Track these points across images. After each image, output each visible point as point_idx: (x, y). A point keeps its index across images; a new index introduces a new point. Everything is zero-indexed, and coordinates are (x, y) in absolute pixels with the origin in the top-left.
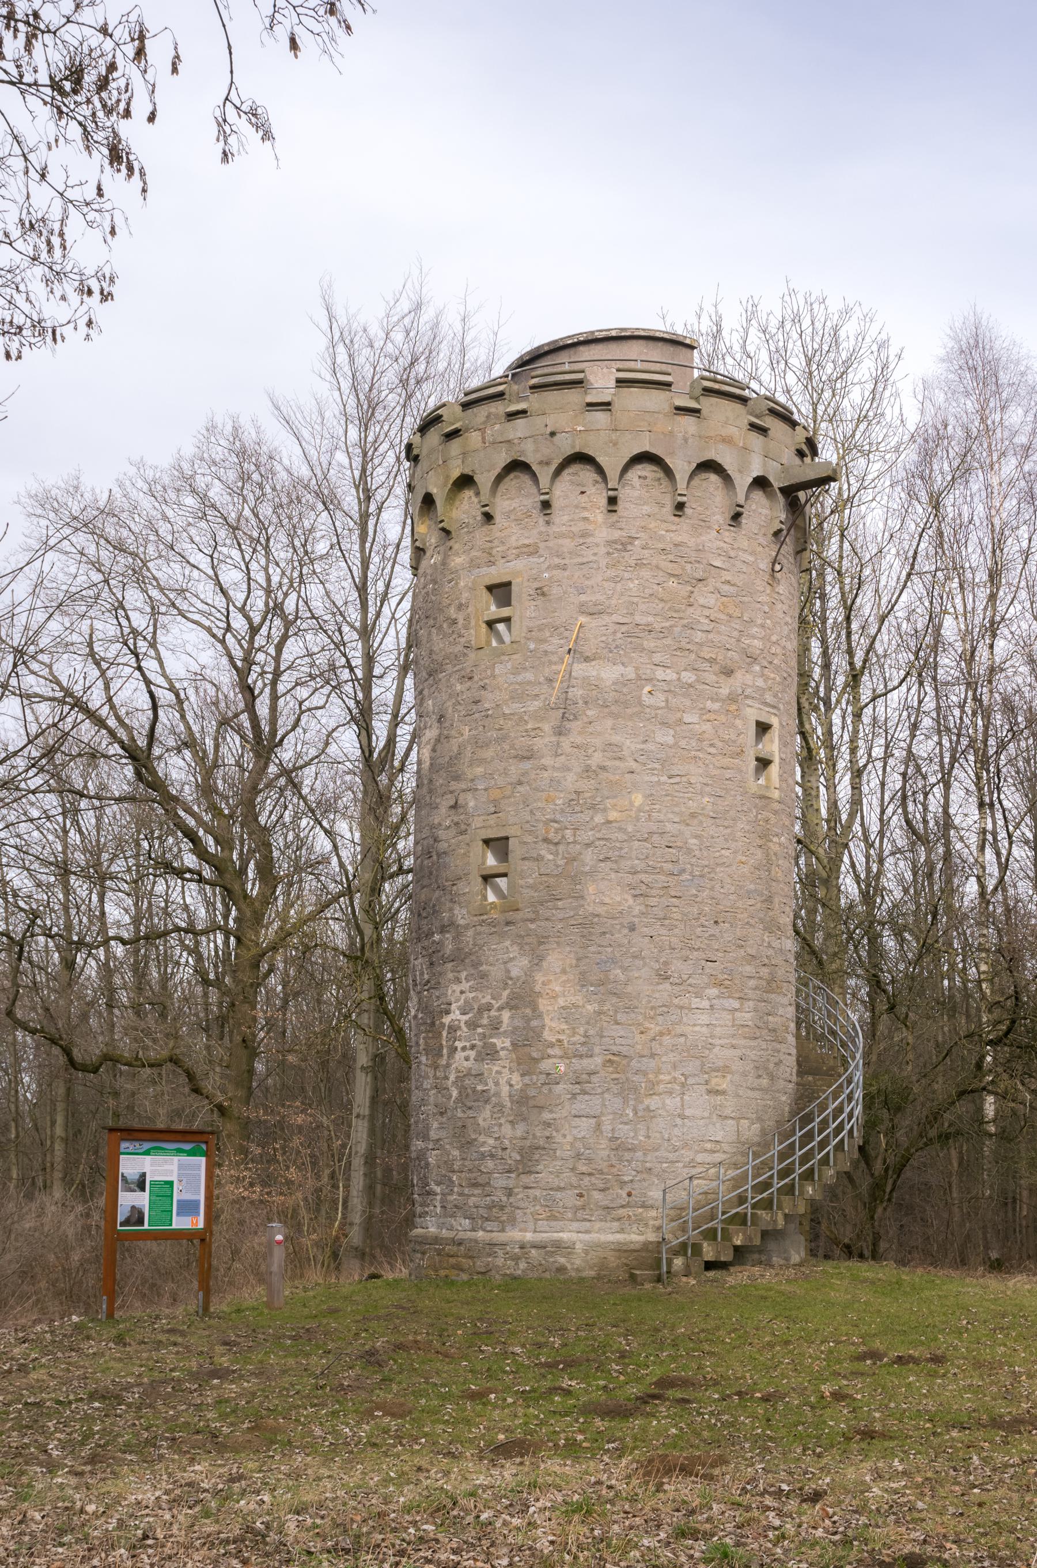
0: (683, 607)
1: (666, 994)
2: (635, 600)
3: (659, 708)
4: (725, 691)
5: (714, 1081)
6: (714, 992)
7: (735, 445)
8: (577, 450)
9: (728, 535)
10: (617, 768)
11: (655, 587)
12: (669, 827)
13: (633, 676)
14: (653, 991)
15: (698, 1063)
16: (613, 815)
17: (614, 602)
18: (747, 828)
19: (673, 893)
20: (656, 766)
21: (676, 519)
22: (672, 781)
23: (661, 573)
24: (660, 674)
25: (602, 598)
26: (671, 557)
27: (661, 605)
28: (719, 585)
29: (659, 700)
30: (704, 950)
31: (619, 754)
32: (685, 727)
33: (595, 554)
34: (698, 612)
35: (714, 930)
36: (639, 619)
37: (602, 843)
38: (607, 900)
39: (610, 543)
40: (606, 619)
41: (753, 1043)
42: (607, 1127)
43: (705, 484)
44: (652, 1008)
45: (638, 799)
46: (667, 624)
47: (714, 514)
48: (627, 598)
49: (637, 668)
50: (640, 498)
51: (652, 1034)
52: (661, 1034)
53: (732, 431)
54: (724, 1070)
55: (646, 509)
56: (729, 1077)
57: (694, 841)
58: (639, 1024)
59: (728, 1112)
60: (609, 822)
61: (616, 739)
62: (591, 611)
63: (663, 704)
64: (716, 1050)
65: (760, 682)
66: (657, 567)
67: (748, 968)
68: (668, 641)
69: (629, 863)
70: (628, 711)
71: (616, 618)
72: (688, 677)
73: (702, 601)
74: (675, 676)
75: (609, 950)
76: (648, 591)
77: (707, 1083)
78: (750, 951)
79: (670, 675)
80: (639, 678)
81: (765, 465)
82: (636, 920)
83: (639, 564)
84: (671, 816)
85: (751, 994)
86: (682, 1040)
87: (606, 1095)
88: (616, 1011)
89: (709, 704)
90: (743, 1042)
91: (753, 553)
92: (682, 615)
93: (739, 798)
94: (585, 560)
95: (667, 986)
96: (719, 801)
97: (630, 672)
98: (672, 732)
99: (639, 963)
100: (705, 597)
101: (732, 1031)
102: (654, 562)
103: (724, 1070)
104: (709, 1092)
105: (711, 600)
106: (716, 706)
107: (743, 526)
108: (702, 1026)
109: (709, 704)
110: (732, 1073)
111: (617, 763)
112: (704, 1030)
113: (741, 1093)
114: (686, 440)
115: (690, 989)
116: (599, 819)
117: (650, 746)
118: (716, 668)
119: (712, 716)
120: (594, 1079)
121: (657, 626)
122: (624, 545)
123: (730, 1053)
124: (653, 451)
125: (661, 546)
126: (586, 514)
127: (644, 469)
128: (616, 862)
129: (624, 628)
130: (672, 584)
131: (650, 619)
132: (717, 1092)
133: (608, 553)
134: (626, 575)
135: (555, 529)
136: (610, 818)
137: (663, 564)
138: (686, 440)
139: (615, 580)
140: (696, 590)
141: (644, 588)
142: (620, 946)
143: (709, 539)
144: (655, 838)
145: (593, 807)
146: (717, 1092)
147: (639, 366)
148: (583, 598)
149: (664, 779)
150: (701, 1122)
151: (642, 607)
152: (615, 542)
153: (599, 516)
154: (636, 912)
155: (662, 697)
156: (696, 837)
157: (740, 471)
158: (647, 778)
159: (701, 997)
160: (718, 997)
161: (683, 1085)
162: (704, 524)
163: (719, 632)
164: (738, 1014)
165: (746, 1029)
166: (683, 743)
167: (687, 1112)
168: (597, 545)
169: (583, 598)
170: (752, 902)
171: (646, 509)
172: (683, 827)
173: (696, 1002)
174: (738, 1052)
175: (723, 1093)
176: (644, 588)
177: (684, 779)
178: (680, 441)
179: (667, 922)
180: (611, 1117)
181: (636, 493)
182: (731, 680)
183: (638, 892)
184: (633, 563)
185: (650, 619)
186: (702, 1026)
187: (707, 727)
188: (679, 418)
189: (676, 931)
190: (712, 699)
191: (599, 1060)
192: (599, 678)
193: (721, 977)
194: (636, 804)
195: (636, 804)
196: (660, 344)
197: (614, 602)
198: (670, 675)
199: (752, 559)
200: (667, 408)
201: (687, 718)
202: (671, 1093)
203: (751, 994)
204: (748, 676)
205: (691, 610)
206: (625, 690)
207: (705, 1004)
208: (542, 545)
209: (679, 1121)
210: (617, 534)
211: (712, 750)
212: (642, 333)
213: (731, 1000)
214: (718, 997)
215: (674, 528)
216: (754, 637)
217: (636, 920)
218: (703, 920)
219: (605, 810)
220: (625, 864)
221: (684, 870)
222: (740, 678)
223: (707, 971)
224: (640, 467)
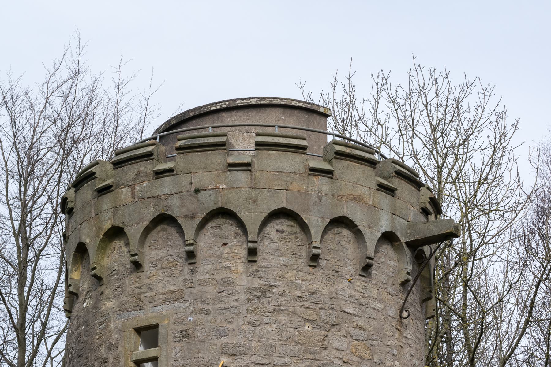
2: (274, 342)
7: (365, 203)
8: (220, 205)
9: (359, 285)
11: (292, 331)
17: (253, 344)
21: (311, 269)
23: (297, 319)
25: (243, 340)
26: (307, 304)
27: (297, 347)
28: (351, 329)
33: (236, 300)
34: (332, 354)
39: (250, 290)
40: (246, 360)
43: (337, 238)
47: (346, 265)
48: (265, 341)
50: (278, 250)
53: (362, 190)
55: (284, 260)
62: (232, 352)
66: (294, 313)
71: (255, 359)
73: (335, 344)
81: (392, 221)
83: (277, 310)
91: (382, 301)
92: (317, 356)
94: (227, 305)
100: (338, 341)
102: (291, 308)
105: (344, 344)
107: (373, 276)
114: (320, 198)
122: (264, 292)
124: (290, 207)
125: (296, 293)
126: (228, 264)
127: (281, 224)
130: (307, 328)
133: (248, 300)
134: (265, 320)
135: (198, 277)
137: (299, 310)
138: (320, 198)
139: (255, 324)
140: (330, 334)
141: (282, 331)
143: (341, 287)
147: (277, 131)
148: (225, 340)
151: (280, 349)
152: (255, 289)
153: (240, 266)
157: (369, 227)
162: (338, 274)
168: (238, 292)
169: (225, 340)
171: (284, 260)
176: (282, 331)
178: (314, 199)
181: (274, 246)
184: (271, 309)
188: (314, 179)
196: (296, 112)
197: (253, 344)
199: (381, 306)
200: (302, 169)
205: (325, 352)
208: (187, 291)
210: (256, 282)
212: (280, 102)
215: (309, 277)
224: (278, 221)
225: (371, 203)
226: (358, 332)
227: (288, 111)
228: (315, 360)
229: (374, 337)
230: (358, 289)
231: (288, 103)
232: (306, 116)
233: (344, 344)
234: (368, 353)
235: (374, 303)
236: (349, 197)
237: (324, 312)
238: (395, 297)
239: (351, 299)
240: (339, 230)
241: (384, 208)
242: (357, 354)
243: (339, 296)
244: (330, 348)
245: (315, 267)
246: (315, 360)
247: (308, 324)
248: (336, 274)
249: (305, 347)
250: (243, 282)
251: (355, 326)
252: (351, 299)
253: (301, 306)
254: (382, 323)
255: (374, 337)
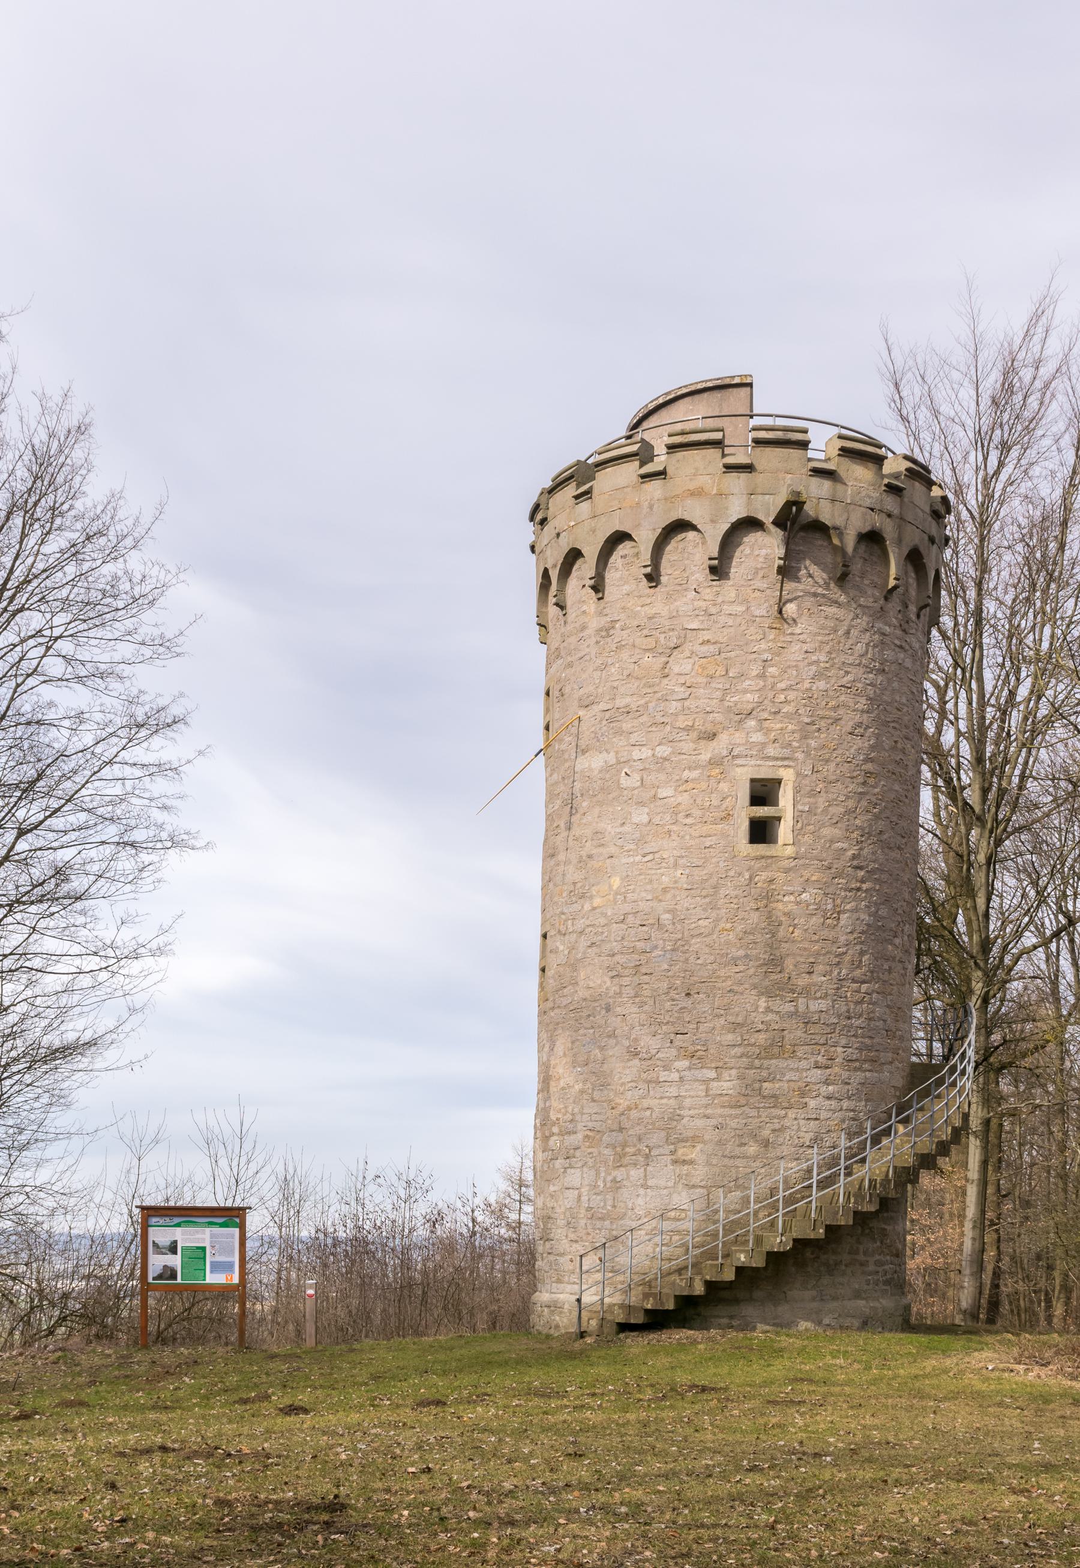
0: (657, 680)
1: (635, 1069)
2: (615, 684)
3: (635, 789)
4: (705, 756)
5: (680, 1152)
6: (686, 1063)
9: (710, 590)
10: (601, 854)
11: (632, 666)
12: (642, 905)
13: (614, 761)
14: (624, 1068)
15: (663, 1134)
16: (597, 901)
17: (600, 690)
18: (733, 893)
19: (644, 971)
20: (632, 847)
22: (646, 859)
23: (637, 651)
24: (636, 754)
26: (645, 632)
29: (634, 781)
30: (673, 1023)
31: (602, 841)
32: (660, 803)
34: (673, 682)
35: (688, 1003)
36: (620, 702)
37: (590, 929)
38: (592, 984)
41: (733, 1112)
42: (584, 1198)
43: (681, 545)
44: (623, 1084)
45: (616, 882)
46: (642, 702)
47: (692, 574)
48: (609, 684)
49: (617, 753)
50: (621, 578)
51: (621, 1108)
52: (629, 1109)
53: (704, 481)
54: (695, 1139)
55: (626, 588)
56: (699, 1147)
57: (667, 916)
58: (610, 1101)
59: (696, 1181)
60: (594, 909)
61: (602, 826)
62: (586, 703)
63: (639, 784)
64: (685, 1121)
65: (757, 737)
67: (730, 1037)
68: (644, 719)
69: (608, 946)
70: (611, 796)
71: (603, 706)
72: (664, 751)
73: (676, 669)
74: (650, 753)
75: (592, 1031)
76: (626, 673)
77: (673, 1153)
78: (731, 1019)
79: (646, 753)
80: (619, 762)
81: (749, 503)
82: (611, 1000)
83: (620, 647)
84: (644, 894)
85: (732, 1062)
86: (648, 1113)
87: (585, 1169)
88: (593, 1089)
89: (686, 774)
90: (720, 1111)
92: (656, 689)
93: (722, 864)
95: (636, 1062)
96: (696, 871)
97: (611, 758)
98: (646, 810)
99: (612, 1041)
100: (681, 665)
101: (704, 1101)
103: (695, 1139)
104: (675, 1162)
106: (695, 774)
108: (669, 1098)
109: (686, 774)
110: (704, 1142)
111: (601, 850)
112: (672, 1102)
113: (714, 1162)
114: (651, 507)
115: (659, 1063)
116: (587, 907)
117: (627, 828)
118: (694, 735)
119: (690, 785)
120: (578, 1153)
121: (634, 707)
123: (700, 1123)
125: (636, 623)
127: (624, 548)
128: (599, 946)
129: (608, 715)
130: (647, 659)
131: (628, 700)
132: (684, 1162)
133: (597, 642)
136: (595, 905)
137: (639, 641)
138: (651, 507)
141: (623, 669)
142: (600, 1027)
143: (685, 603)
144: (630, 919)
145: (582, 896)
146: (684, 1162)
149: (638, 858)
150: (665, 1192)
151: (622, 690)
152: (601, 630)
154: (611, 993)
155: (636, 777)
156: (669, 912)
157: (713, 521)
158: (624, 861)
159: (669, 1070)
160: (690, 1068)
161: (647, 1156)
162: (682, 586)
163: (696, 698)
164: (715, 1084)
165: (726, 1098)
166: (657, 820)
167: (650, 1183)
170: (742, 968)
172: (655, 904)
173: (663, 1076)
174: (714, 1122)
175: (691, 1162)
176: (623, 669)
177: (657, 855)
178: (646, 510)
179: (637, 1000)
180: (587, 1188)
182: (714, 743)
183: (614, 973)
185: (628, 700)
186: (669, 1098)
187: (684, 799)
188: (646, 486)
189: (646, 1008)
190: (690, 768)
191: (580, 1136)
192: (591, 770)
193: (691, 1048)
194: (615, 888)
195: (615, 888)
197: (600, 690)
198: (646, 753)
199: (740, 609)
201: (663, 793)
202: (635, 1165)
203: (732, 1062)
204: (737, 735)
205: (665, 681)
206: (608, 776)
207: (675, 1076)
209: (642, 1191)
211: (689, 821)
213: (705, 1071)
214: (690, 1068)
216: (745, 691)
217: (611, 1000)
218: (673, 994)
219: (591, 897)
220: (606, 948)
221: (656, 947)
222: (724, 738)
223: (677, 1043)
224: (621, 546)
225: (715, 492)
226: (705, 648)
227: (697, 397)
228: (655, 692)
229: (729, 648)
230: (707, 598)
231: (693, 388)
232: (717, 395)
233: (687, 667)
234: (720, 669)
235: (730, 608)
236: (685, 495)
237: (663, 636)
238: (768, 592)
239: (697, 612)
240: (683, 535)
241: (735, 491)
242: (706, 673)
243: (680, 613)
244: (672, 675)
245: (655, 587)
246: (655, 692)
247: (647, 654)
248: (679, 588)
249: (644, 681)
250: (594, 624)
251: (701, 641)
252: (697, 612)
253: (640, 636)
254: (744, 628)
255: (729, 648)
